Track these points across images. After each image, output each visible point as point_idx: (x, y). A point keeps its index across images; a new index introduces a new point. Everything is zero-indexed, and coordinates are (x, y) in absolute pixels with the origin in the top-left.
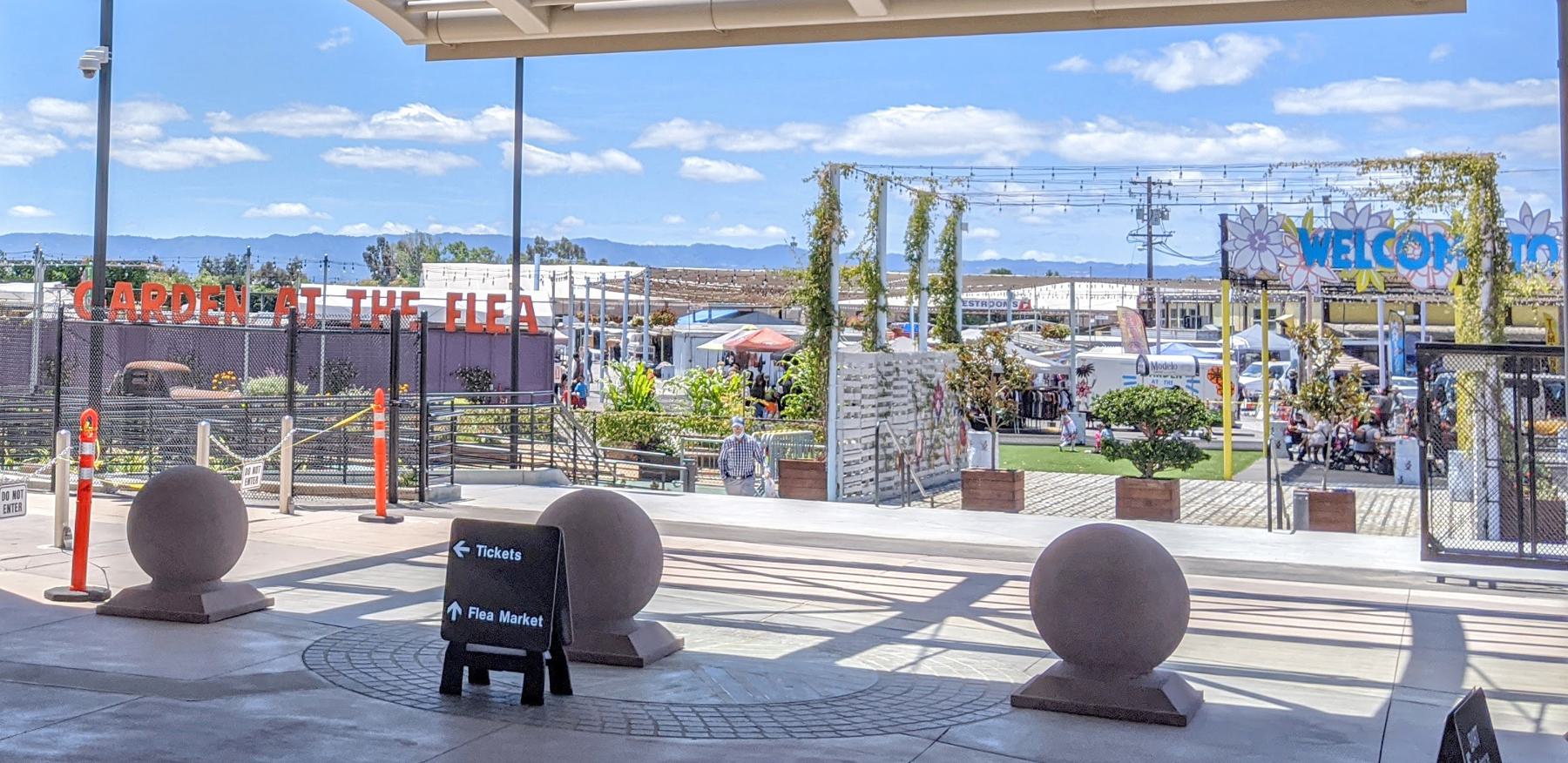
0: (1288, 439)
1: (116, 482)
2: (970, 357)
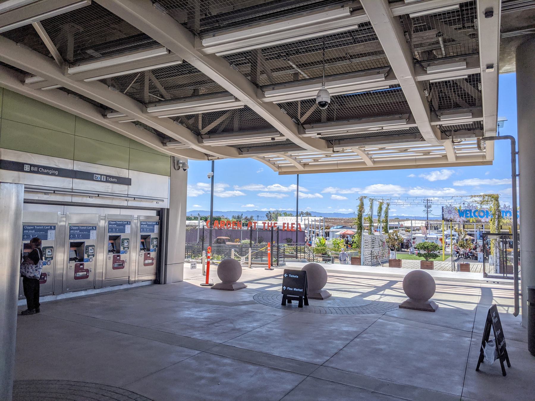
0: (456, 253)
1: (215, 262)
2: (390, 236)
